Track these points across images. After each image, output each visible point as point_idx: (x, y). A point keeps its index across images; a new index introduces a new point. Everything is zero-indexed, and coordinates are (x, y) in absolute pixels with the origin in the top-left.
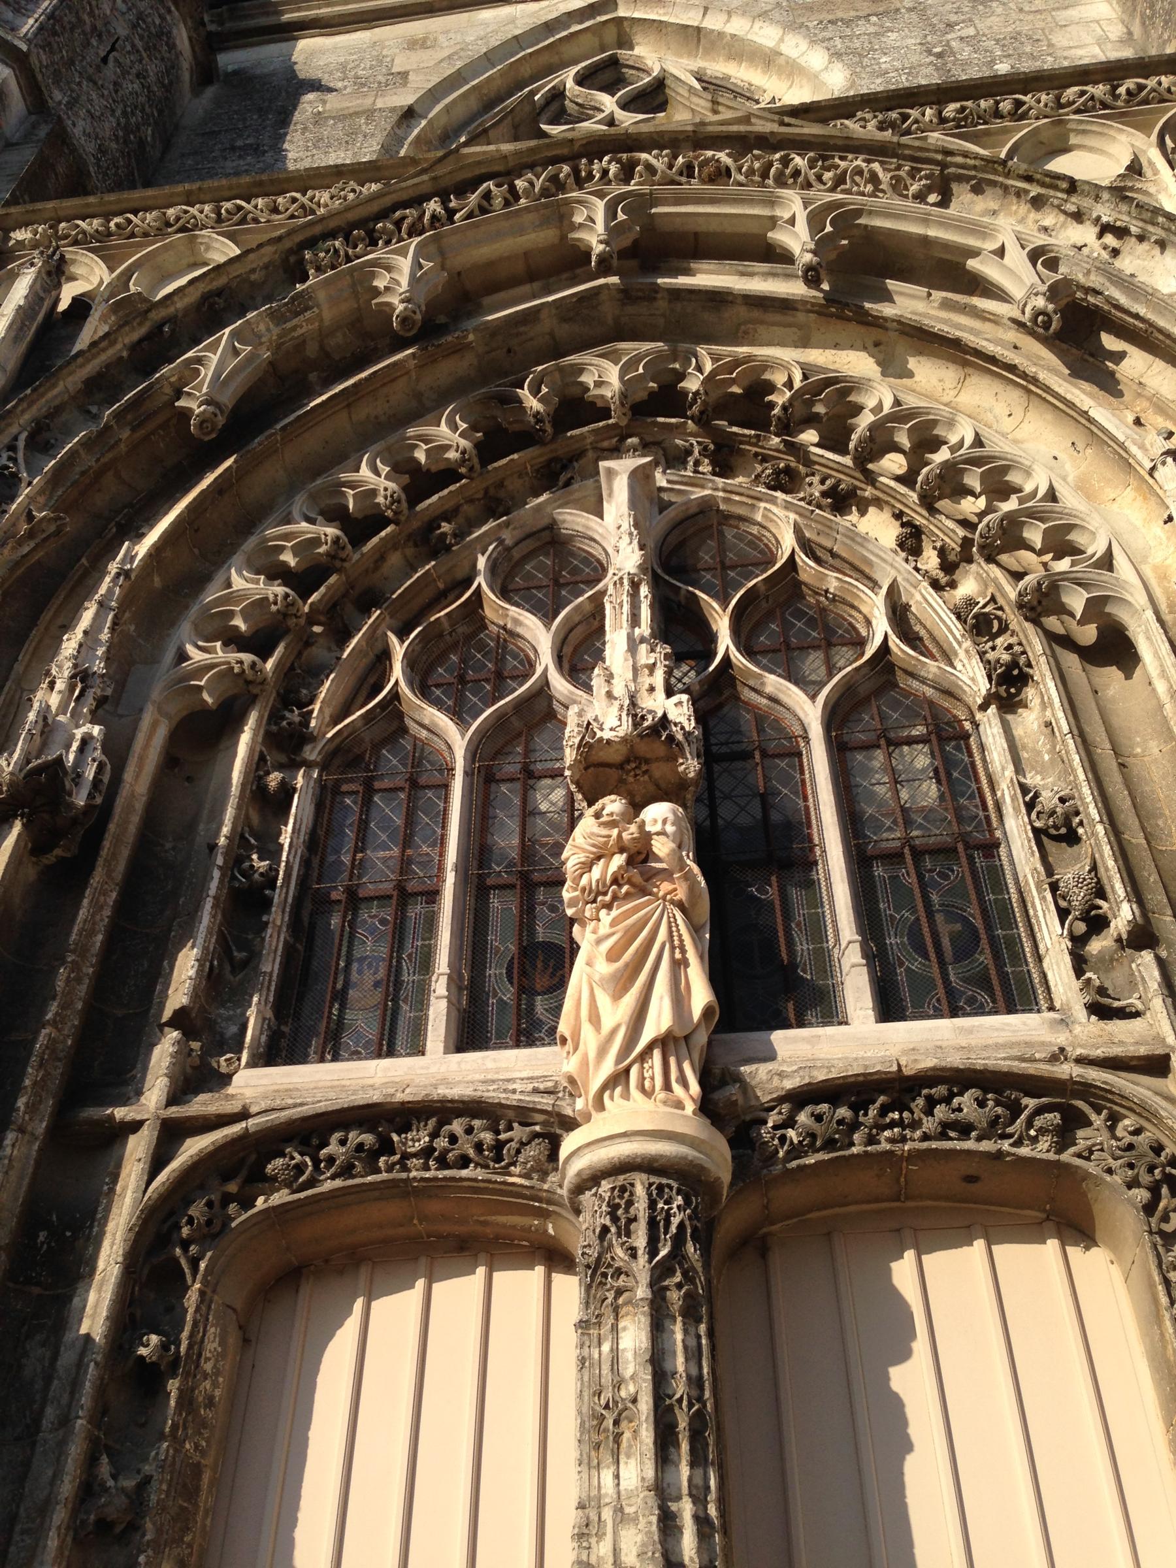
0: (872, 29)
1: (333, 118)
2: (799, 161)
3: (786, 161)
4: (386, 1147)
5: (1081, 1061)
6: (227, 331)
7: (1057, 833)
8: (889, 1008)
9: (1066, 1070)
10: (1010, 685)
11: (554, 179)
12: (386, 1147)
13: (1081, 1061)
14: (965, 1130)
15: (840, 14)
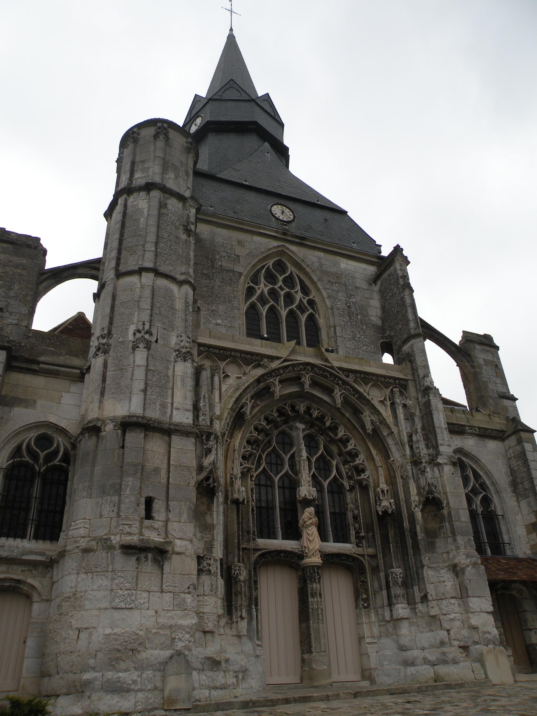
0: (336, 289)
1: (225, 270)
2: (340, 382)
3: (338, 381)
4: (279, 555)
5: (357, 554)
6: (249, 395)
7: (355, 518)
8: (334, 542)
9: (355, 555)
10: (352, 488)
11: (300, 369)
12: (279, 555)
13: (357, 554)
14: (342, 560)
15: (330, 279)
